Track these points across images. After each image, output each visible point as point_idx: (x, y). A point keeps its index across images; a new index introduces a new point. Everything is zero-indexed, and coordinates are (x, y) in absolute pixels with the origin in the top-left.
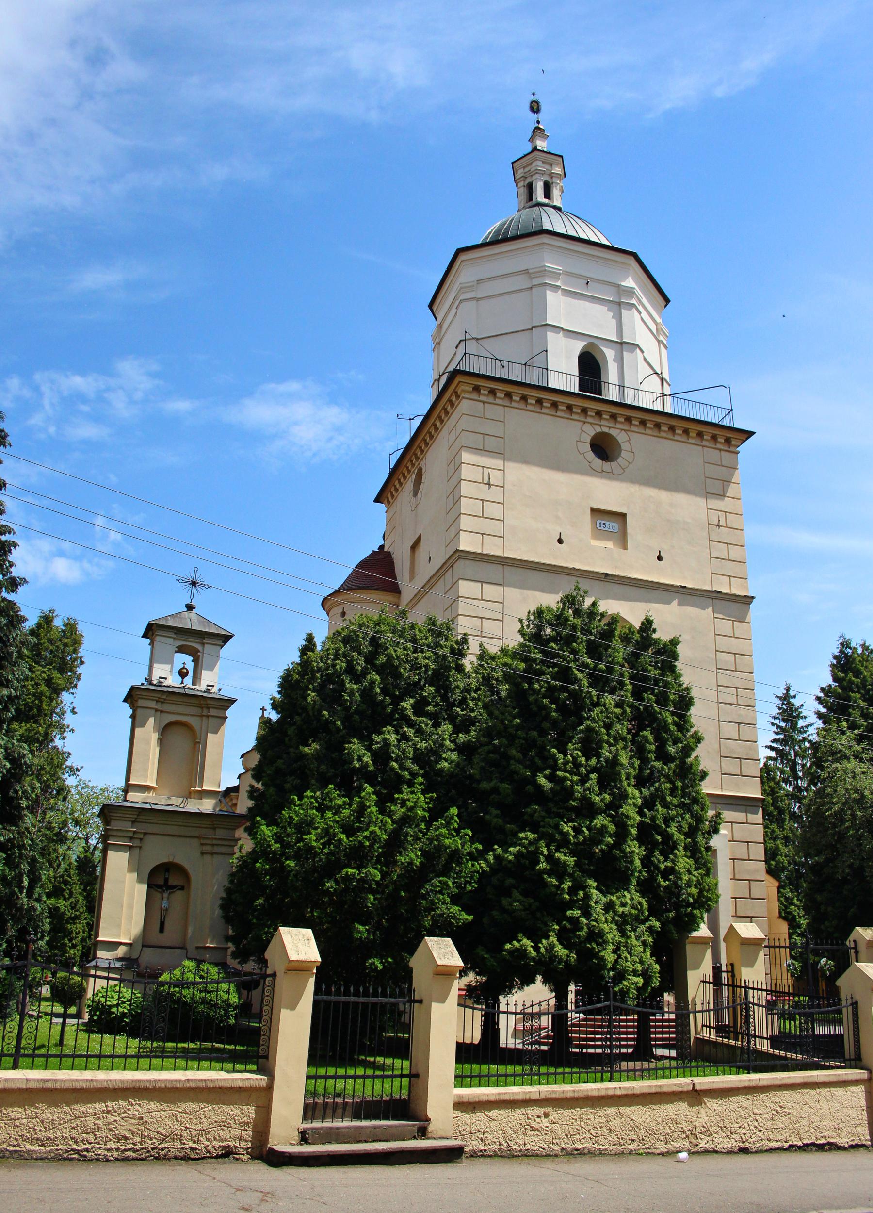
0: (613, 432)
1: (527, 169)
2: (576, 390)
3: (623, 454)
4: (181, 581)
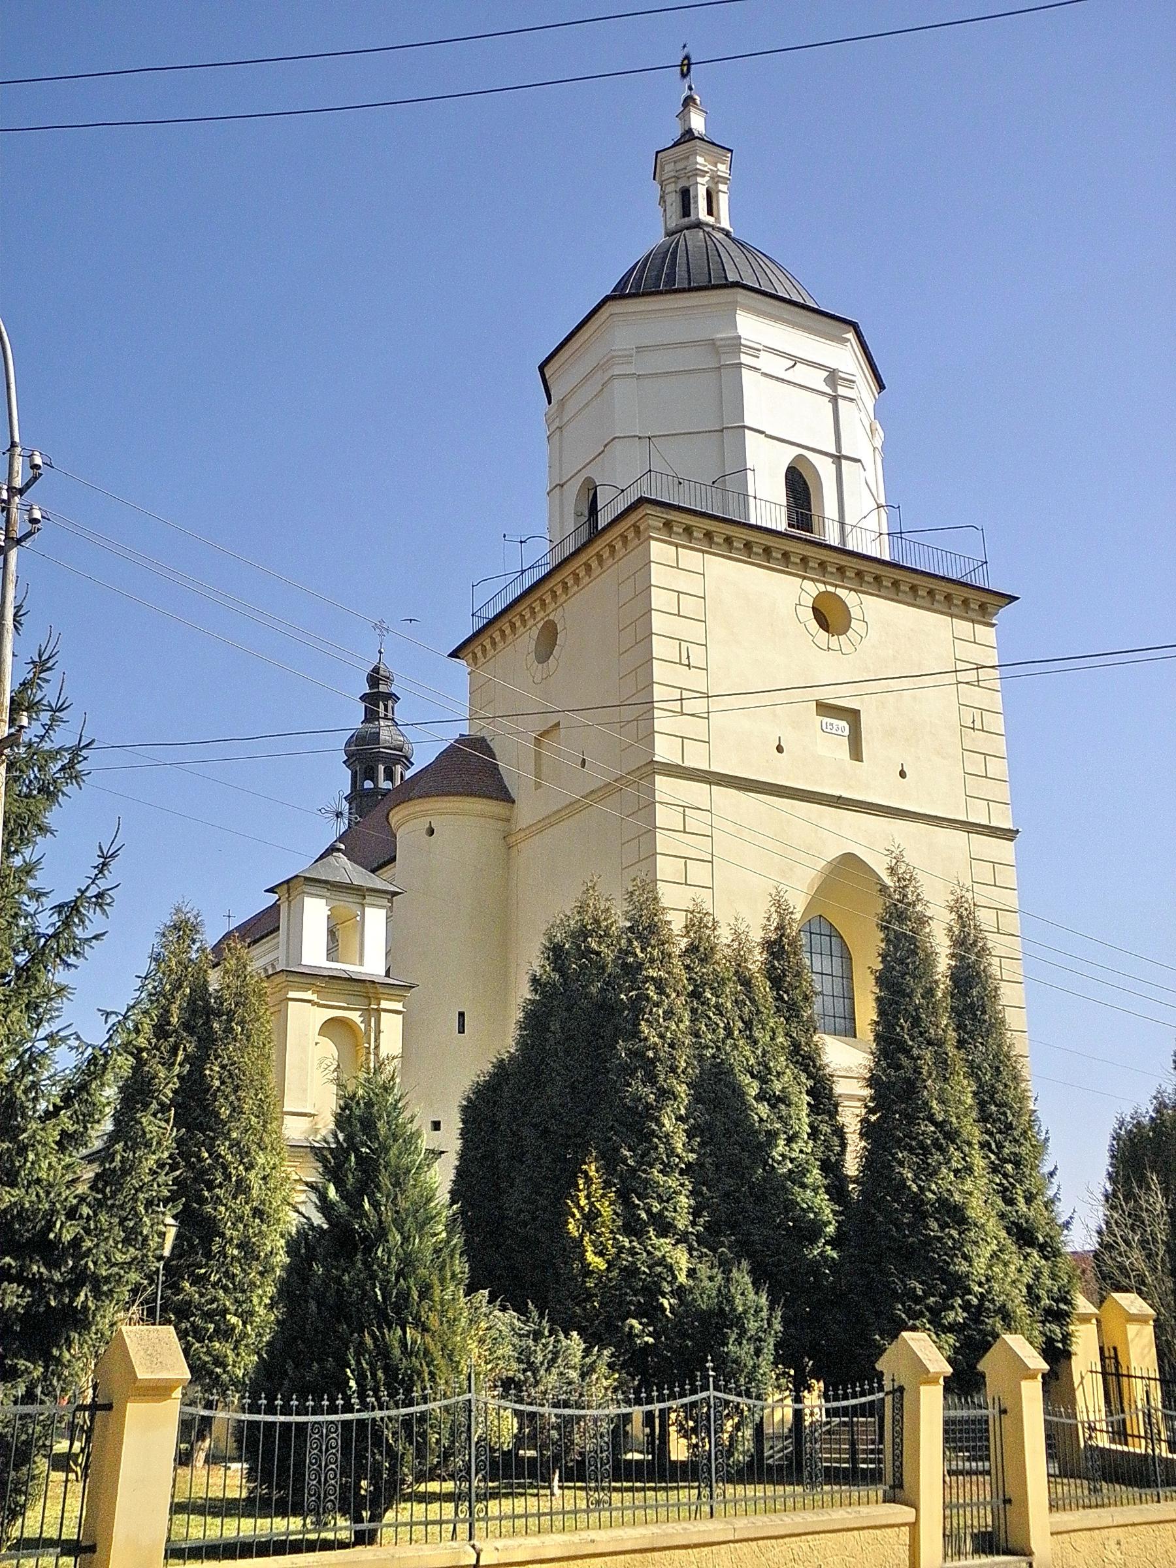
0: (841, 593)
1: (680, 166)
2: (781, 524)
3: (854, 623)
4: (323, 811)
